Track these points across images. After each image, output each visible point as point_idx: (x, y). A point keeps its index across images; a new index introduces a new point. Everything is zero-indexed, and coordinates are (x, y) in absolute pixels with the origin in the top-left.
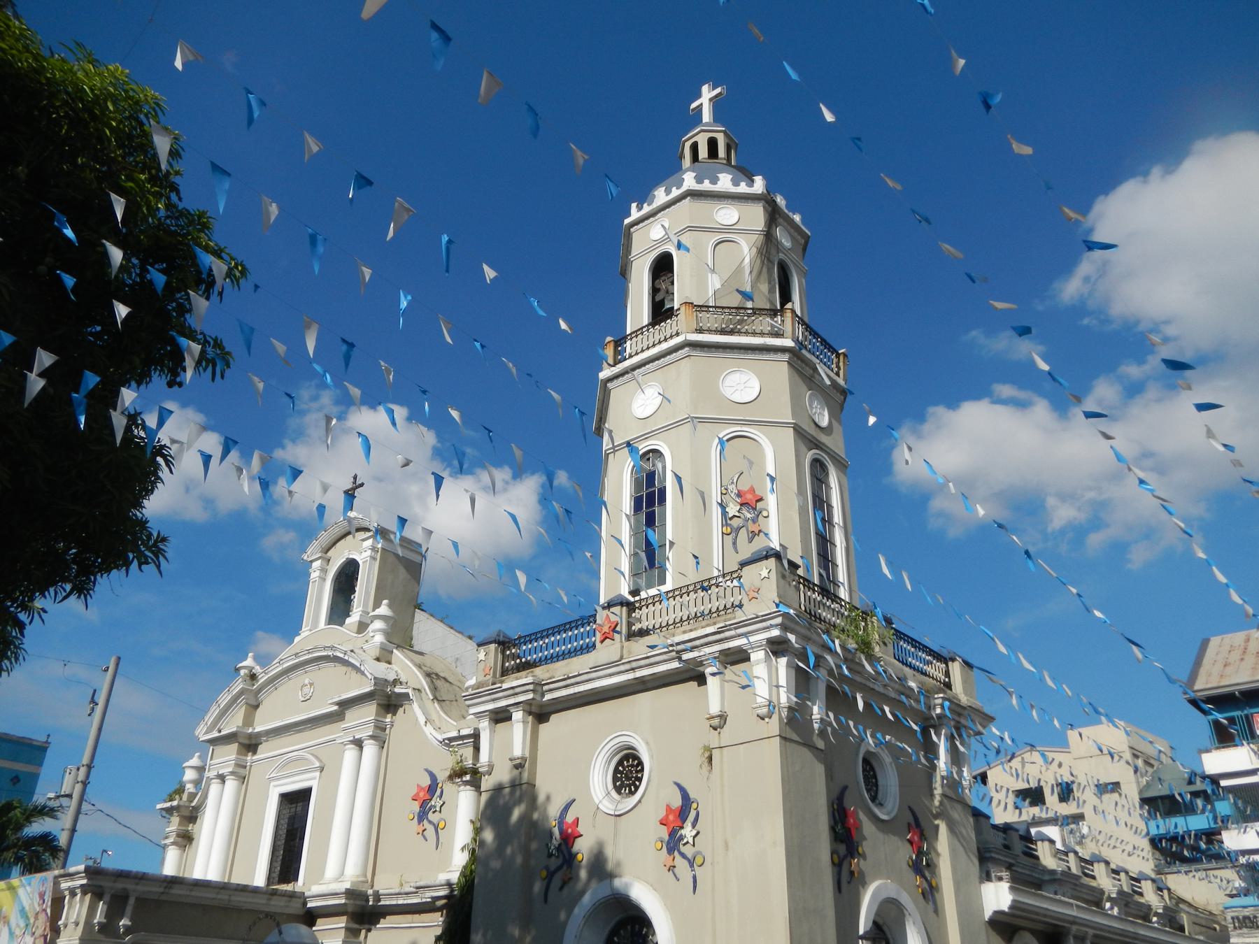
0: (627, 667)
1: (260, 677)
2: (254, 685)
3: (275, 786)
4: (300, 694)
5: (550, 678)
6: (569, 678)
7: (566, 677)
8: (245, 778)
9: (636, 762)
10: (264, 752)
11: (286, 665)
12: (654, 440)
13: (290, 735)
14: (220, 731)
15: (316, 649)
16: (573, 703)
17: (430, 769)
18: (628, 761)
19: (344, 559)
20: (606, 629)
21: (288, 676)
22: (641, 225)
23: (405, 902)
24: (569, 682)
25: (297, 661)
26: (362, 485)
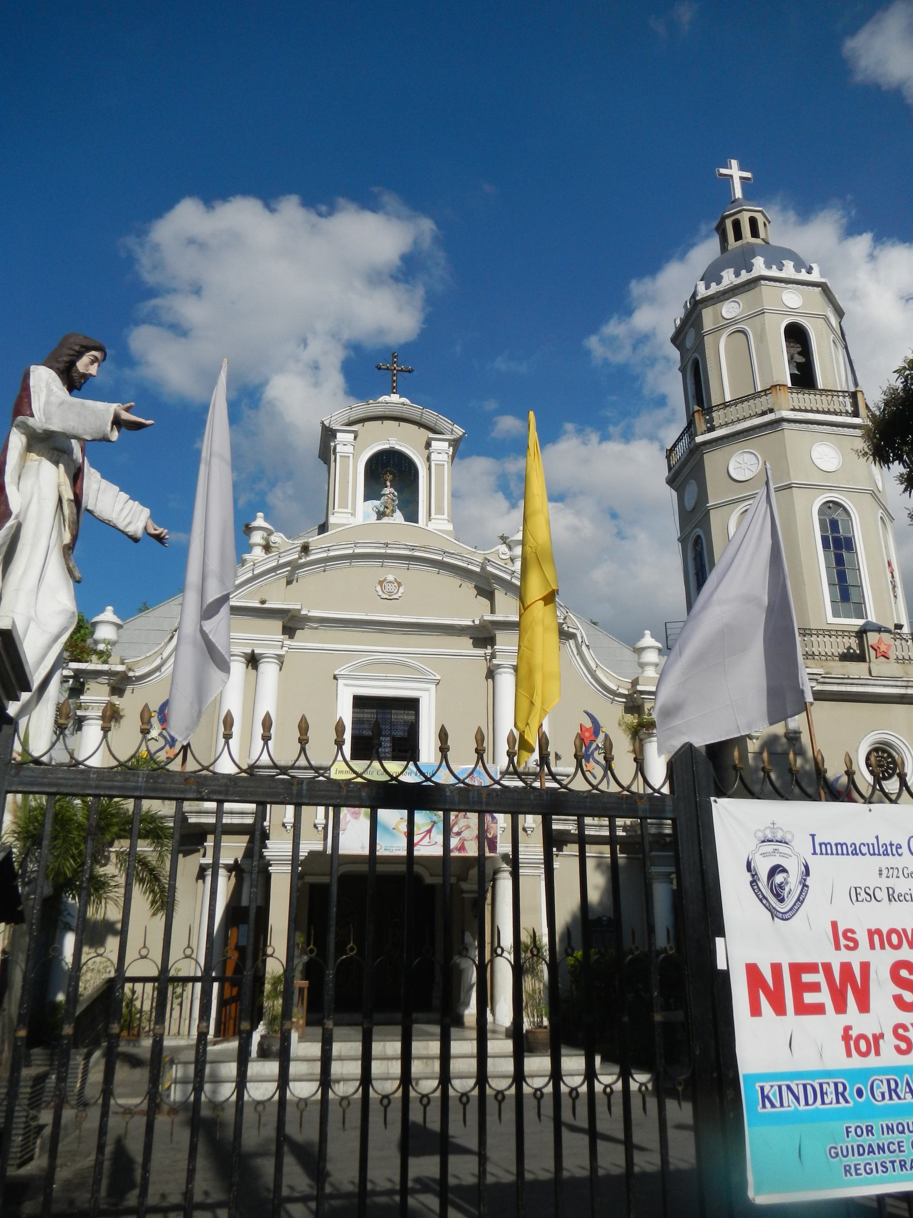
0: (904, 684)
1: (313, 552)
2: (300, 558)
3: (346, 685)
4: (379, 588)
5: (827, 674)
6: (848, 678)
7: (846, 677)
8: (282, 663)
9: (886, 755)
10: (304, 640)
11: (357, 551)
12: (841, 495)
13: (365, 631)
14: (263, 602)
15: (424, 548)
16: (830, 697)
17: (590, 712)
18: (877, 752)
19: (387, 446)
20: (883, 648)
21: (350, 563)
22: (772, 283)
23: (597, 833)
24: (846, 681)
25: (383, 551)
26: (409, 371)
